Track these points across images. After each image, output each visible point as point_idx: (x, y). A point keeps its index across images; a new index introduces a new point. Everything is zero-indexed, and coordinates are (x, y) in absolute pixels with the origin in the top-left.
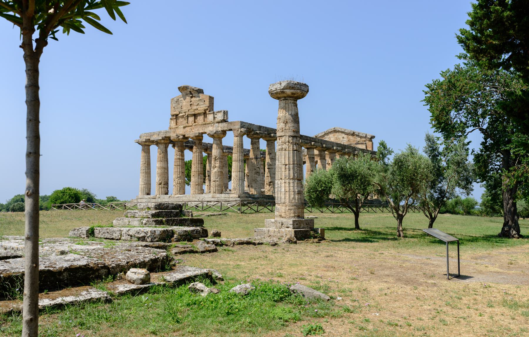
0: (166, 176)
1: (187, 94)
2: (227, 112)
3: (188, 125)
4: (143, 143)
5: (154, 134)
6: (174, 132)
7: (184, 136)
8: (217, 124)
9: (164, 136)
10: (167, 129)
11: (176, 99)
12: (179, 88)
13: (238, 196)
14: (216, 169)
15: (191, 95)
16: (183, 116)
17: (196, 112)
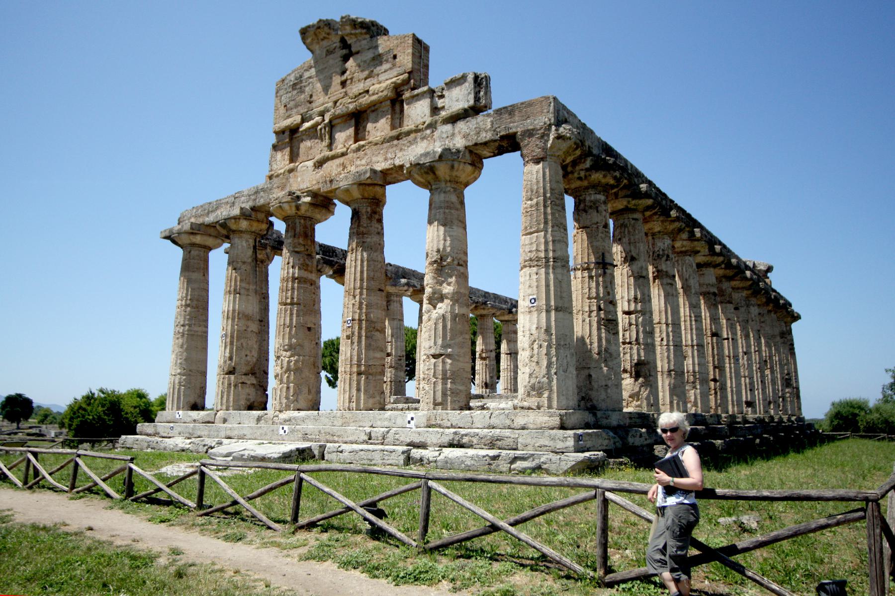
0: (253, 342)
1: (329, 52)
2: (487, 78)
3: (330, 154)
4: (185, 239)
5: (218, 205)
6: (283, 187)
7: (314, 194)
8: (448, 127)
9: (247, 206)
10: (261, 181)
11: (292, 78)
12: (304, 32)
13: (556, 421)
14: (443, 307)
15: (344, 52)
16: (314, 127)
17: (365, 100)
